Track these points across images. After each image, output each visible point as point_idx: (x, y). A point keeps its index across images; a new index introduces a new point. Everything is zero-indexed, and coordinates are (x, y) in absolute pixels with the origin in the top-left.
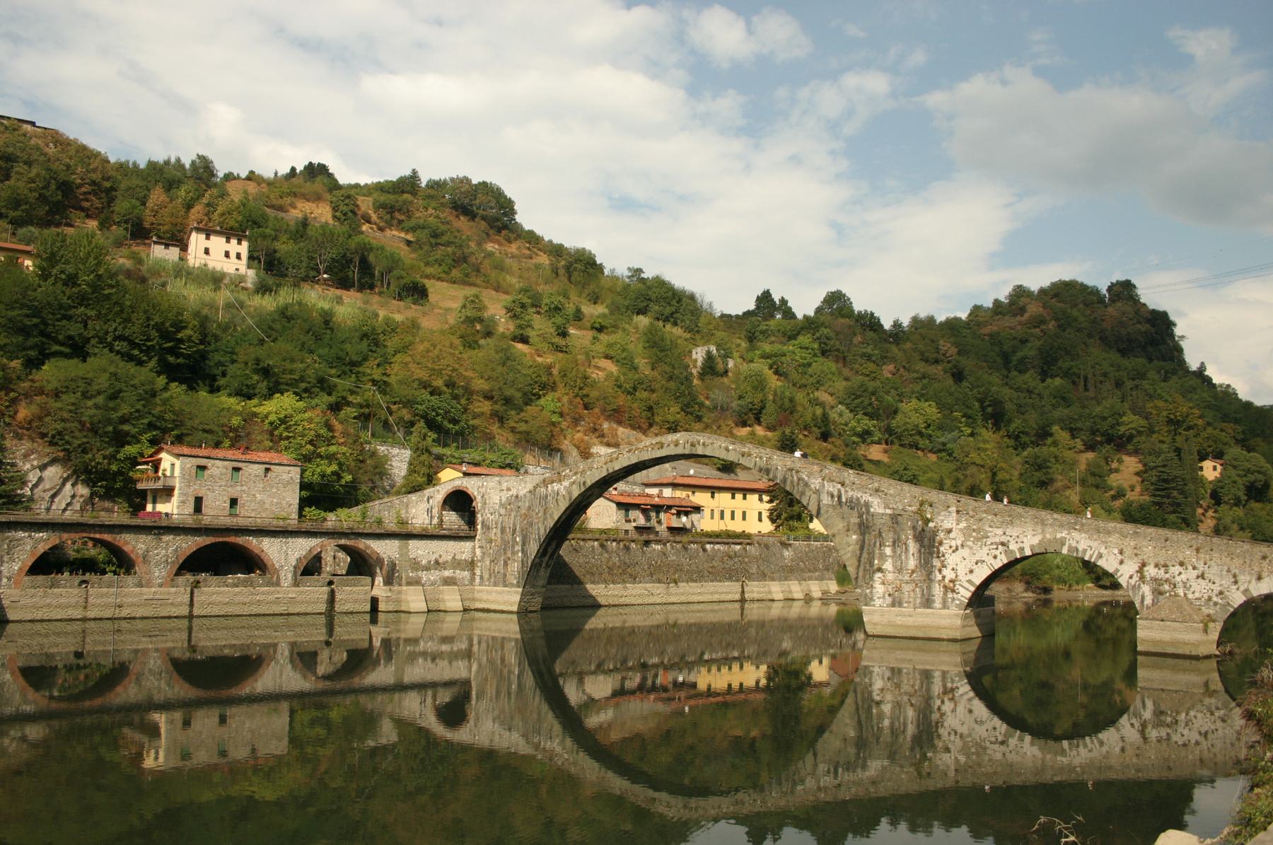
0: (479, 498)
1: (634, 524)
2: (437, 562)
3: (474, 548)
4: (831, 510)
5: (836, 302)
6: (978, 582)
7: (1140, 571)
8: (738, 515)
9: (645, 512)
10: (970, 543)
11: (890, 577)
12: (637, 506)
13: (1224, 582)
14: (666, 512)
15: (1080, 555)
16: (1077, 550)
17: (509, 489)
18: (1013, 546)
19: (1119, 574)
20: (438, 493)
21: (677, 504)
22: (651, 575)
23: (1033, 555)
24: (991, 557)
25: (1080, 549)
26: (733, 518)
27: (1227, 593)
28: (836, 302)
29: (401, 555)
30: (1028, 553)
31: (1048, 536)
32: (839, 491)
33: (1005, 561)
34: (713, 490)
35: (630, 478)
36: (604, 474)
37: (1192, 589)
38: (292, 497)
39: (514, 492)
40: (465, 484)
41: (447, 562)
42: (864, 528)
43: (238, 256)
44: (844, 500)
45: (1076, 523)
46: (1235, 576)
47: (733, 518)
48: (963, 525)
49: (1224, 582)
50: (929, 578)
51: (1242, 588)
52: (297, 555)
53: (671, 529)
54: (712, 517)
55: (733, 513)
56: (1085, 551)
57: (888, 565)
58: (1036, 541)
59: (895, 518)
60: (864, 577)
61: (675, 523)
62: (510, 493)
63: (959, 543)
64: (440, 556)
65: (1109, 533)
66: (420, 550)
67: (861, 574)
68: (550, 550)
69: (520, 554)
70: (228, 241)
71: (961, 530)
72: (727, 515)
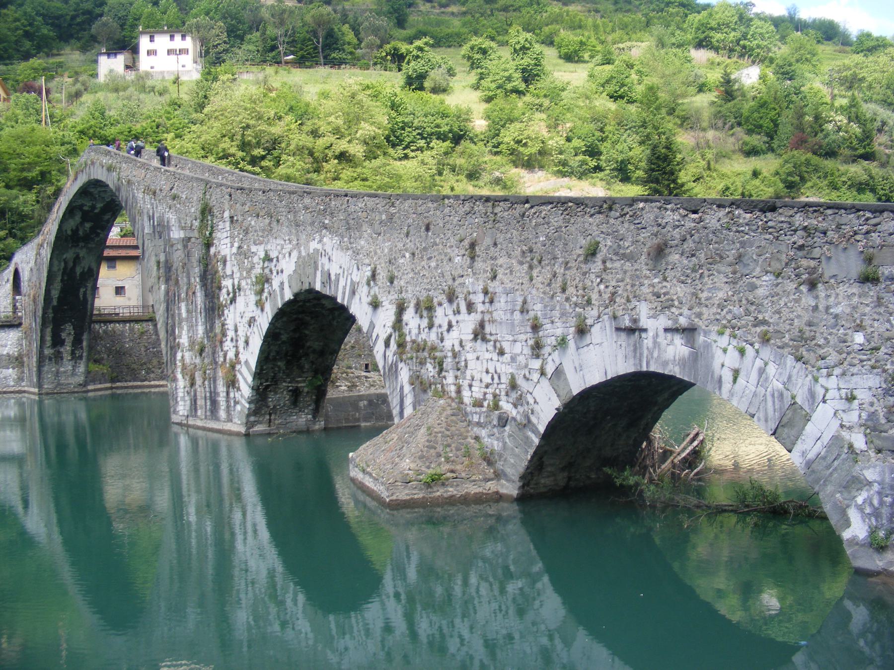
7: (398, 324)
13: (518, 348)
25: (333, 277)
27: (520, 381)
30: (288, 296)
49: (518, 348)
51: (550, 369)
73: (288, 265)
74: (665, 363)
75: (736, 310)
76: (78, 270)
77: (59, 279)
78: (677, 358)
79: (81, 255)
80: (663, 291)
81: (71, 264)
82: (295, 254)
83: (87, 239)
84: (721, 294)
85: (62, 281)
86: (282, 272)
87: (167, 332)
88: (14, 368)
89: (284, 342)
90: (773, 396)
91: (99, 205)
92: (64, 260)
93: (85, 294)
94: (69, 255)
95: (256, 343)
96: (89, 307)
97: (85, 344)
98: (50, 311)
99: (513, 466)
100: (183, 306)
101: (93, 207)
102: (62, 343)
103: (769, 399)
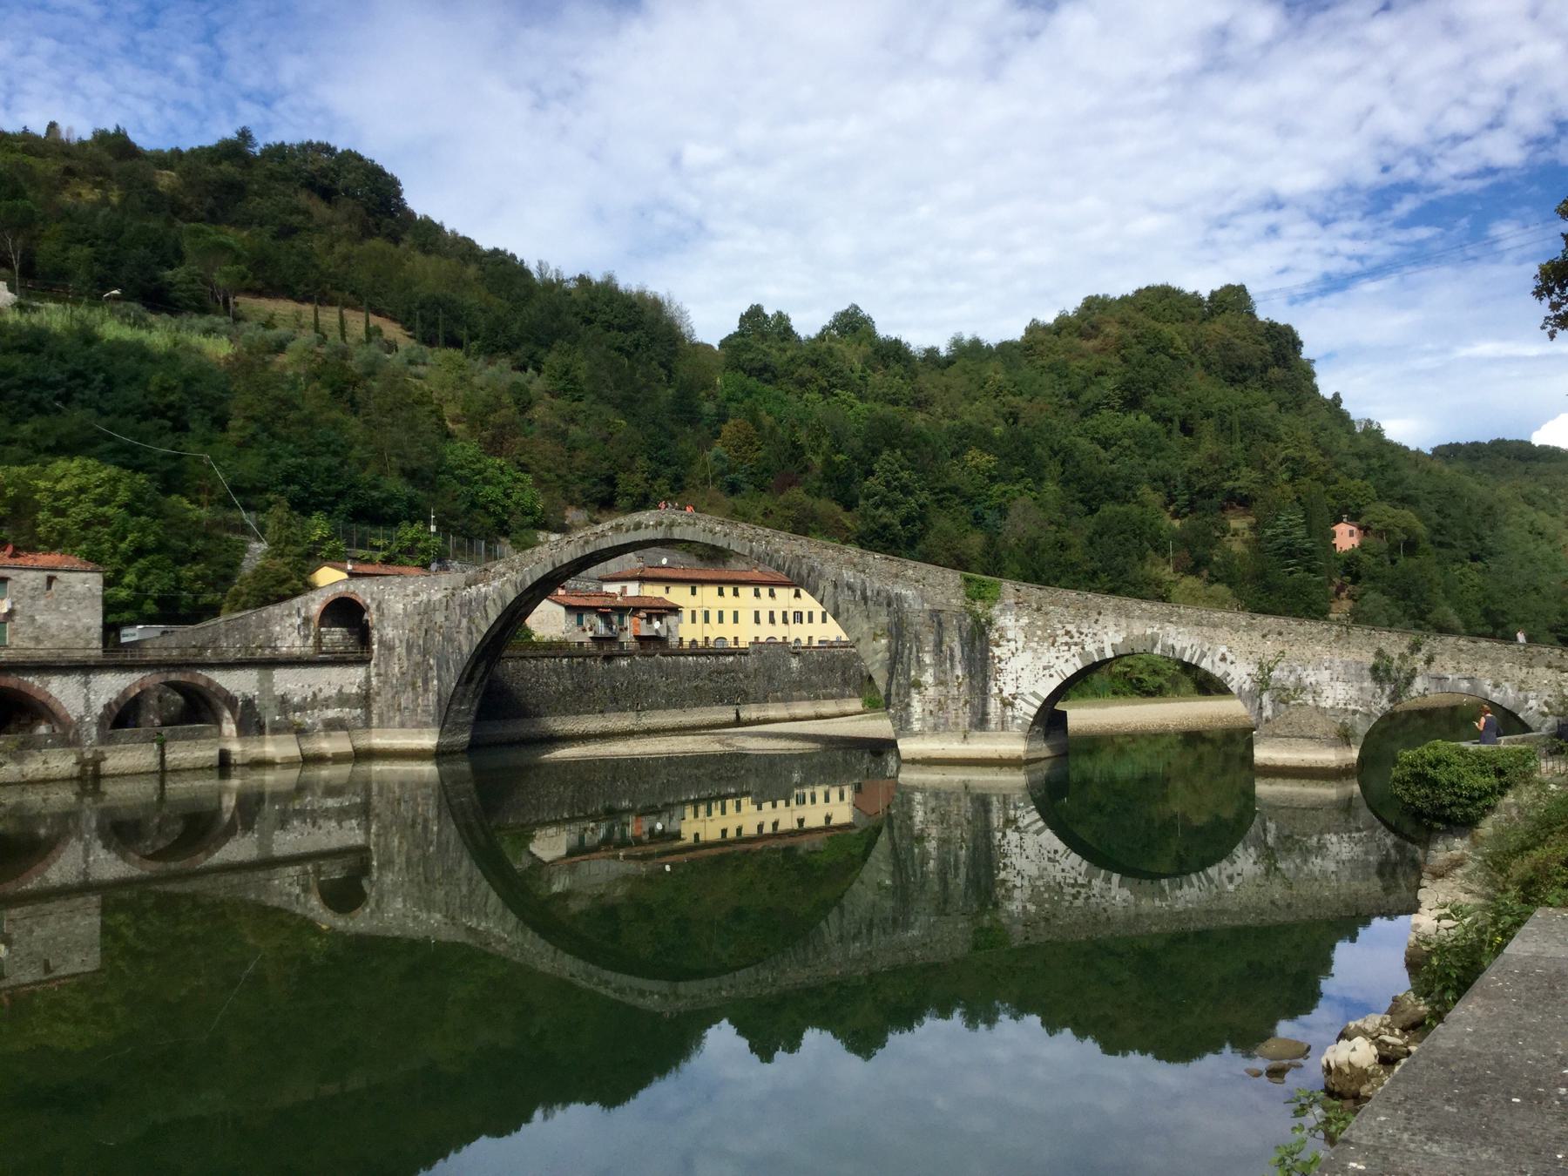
0: (373, 606)
1: (591, 634)
3: (368, 679)
4: (852, 607)
5: (852, 324)
6: (1045, 695)
8: (728, 617)
9: (605, 616)
10: (1034, 645)
11: (931, 692)
12: (593, 609)
14: (633, 615)
15: (1177, 656)
16: (1173, 648)
17: (416, 594)
18: (1091, 647)
19: (1229, 679)
20: (315, 605)
21: (647, 603)
22: (616, 701)
23: (1118, 657)
24: (1062, 660)
25: (1178, 648)
26: (721, 620)
28: (852, 324)
29: (262, 692)
30: (1109, 654)
31: (1136, 632)
32: (863, 583)
33: (1080, 666)
34: (694, 583)
35: (583, 574)
36: (549, 569)
37: (1324, 695)
38: (92, 619)
39: (424, 597)
40: (352, 588)
41: (330, 697)
42: (898, 631)
44: (869, 593)
45: (1171, 614)
47: (721, 620)
48: (1024, 621)
50: (984, 692)
52: (104, 700)
53: (639, 638)
54: (694, 621)
55: (721, 614)
56: (1184, 650)
57: (928, 678)
58: (1119, 640)
59: (935, 614)
60: (898, 695)
61: (645, 631)
62: (419, 599)
63: (1020, 645)
64: (320, 690)
65: (1215, 626)
66: (288, 682)
67: (893, 690)
68: (478, 675)
69: (435, 682)
71: (1022, 628)
72: (714, 617)
82: (1124, 634)
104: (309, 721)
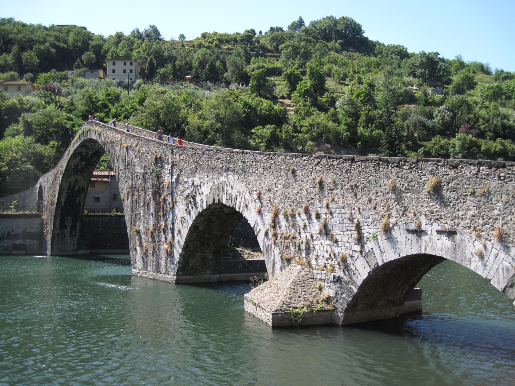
2: (9, 233)
25: (233, 197)
41: (18, 234)
43: (131, 71)
46: (358, 228)
64: (13, 230)
70: (125, 64)
73: (206, 189)
74: (436, 250)
75: (481, 222)
76: (76, 188)
77: (66, 191)
78: (443, 247)
79: (79, 179)
80: (435, 210)
81: (73, 184)
82: (210, 183)
83: (82, 170)
84: (471, 213)
85: (67, 193)
86: (202, 193)
87: (131, 223)
88: (37, 240)
89: (200, 231)
90: (503, 269)
91: (90, 153)
92: (69, 182)
93: (79, 200)
94: (72, 179)
95: (185, 232)
96: (81, 207)
97: (78, 228)
98: (60, 209)
99: (341, 304)
100: (141, 209)
101: (87, 154)
102: (65, 227)
103: (500, 271)
104: (6, 245)
